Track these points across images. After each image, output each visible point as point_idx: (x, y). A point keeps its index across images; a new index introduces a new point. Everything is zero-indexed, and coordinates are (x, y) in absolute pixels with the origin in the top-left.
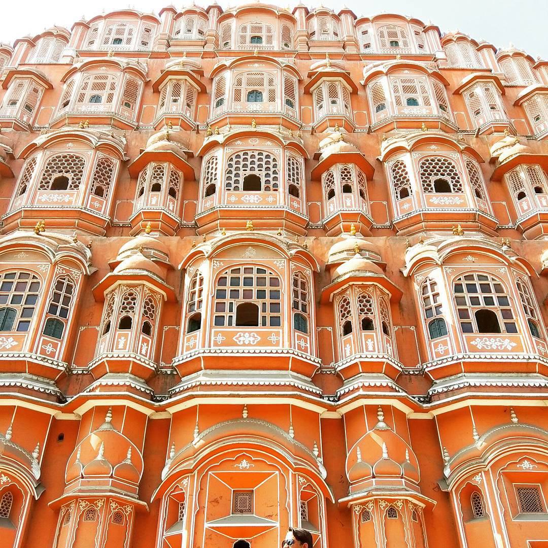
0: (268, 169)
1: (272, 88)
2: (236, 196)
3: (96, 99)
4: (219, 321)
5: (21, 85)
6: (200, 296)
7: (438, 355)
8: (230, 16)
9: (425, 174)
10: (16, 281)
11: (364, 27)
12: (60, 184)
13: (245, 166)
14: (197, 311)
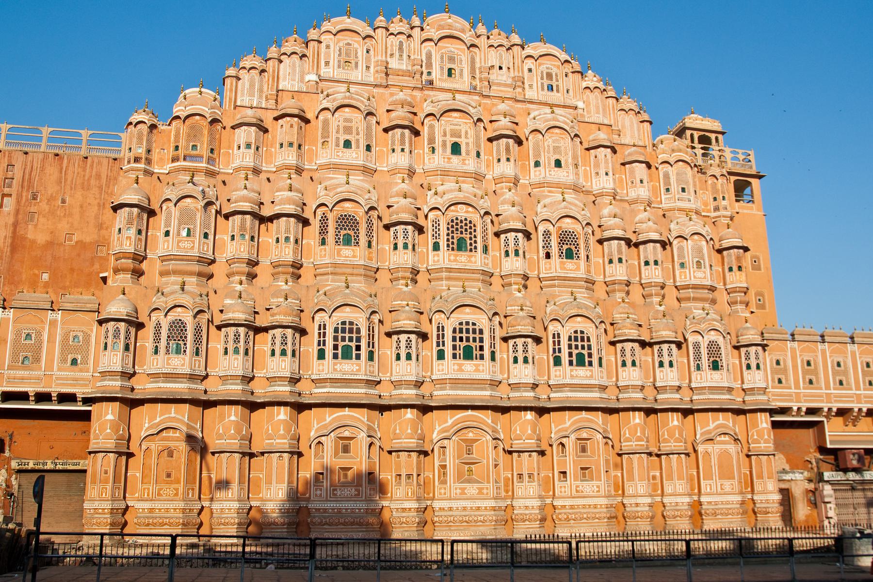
0: (470, 233)
1: (467, 141)
2: (454, 255)
3: (347, 144)
4: (454, 356)
5: (292, 126)
6: (443, 338)
7: (556, 376)
8: (431, 40)
9: (562, 242)
10: (347, 326)
11: (529, 63)
12: (347, 241)
13: (457, 229)
14: (441, 347)
